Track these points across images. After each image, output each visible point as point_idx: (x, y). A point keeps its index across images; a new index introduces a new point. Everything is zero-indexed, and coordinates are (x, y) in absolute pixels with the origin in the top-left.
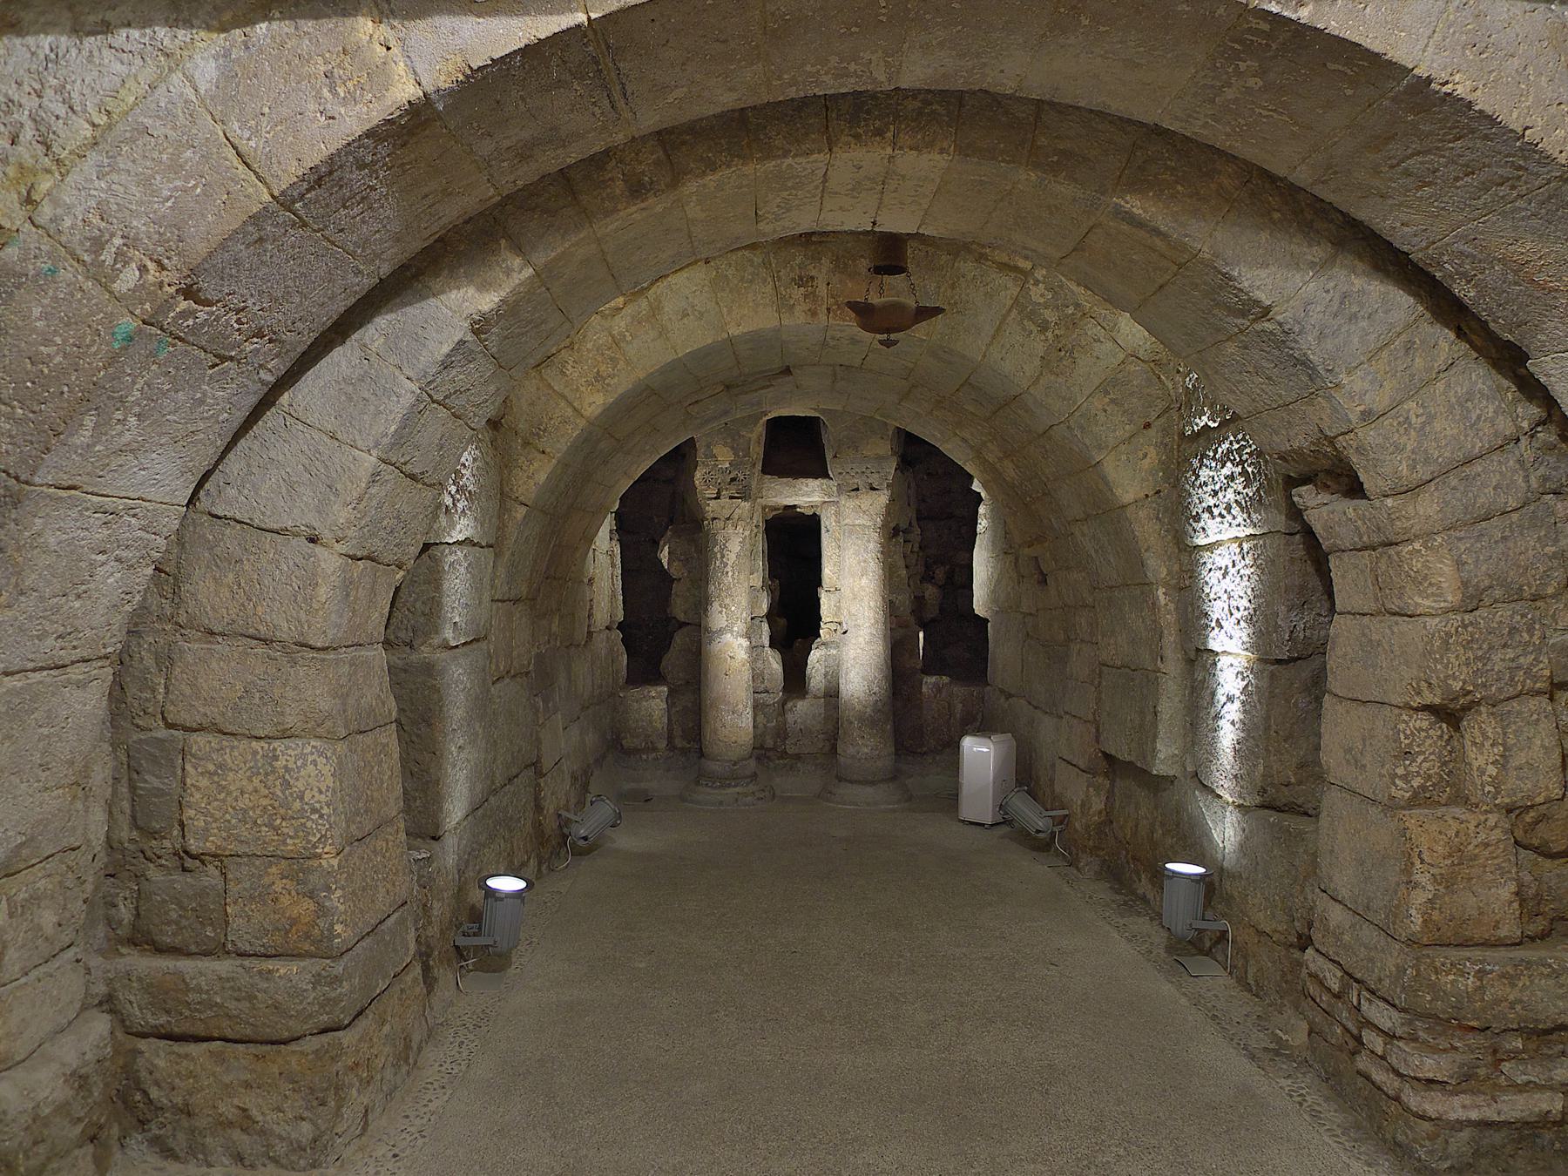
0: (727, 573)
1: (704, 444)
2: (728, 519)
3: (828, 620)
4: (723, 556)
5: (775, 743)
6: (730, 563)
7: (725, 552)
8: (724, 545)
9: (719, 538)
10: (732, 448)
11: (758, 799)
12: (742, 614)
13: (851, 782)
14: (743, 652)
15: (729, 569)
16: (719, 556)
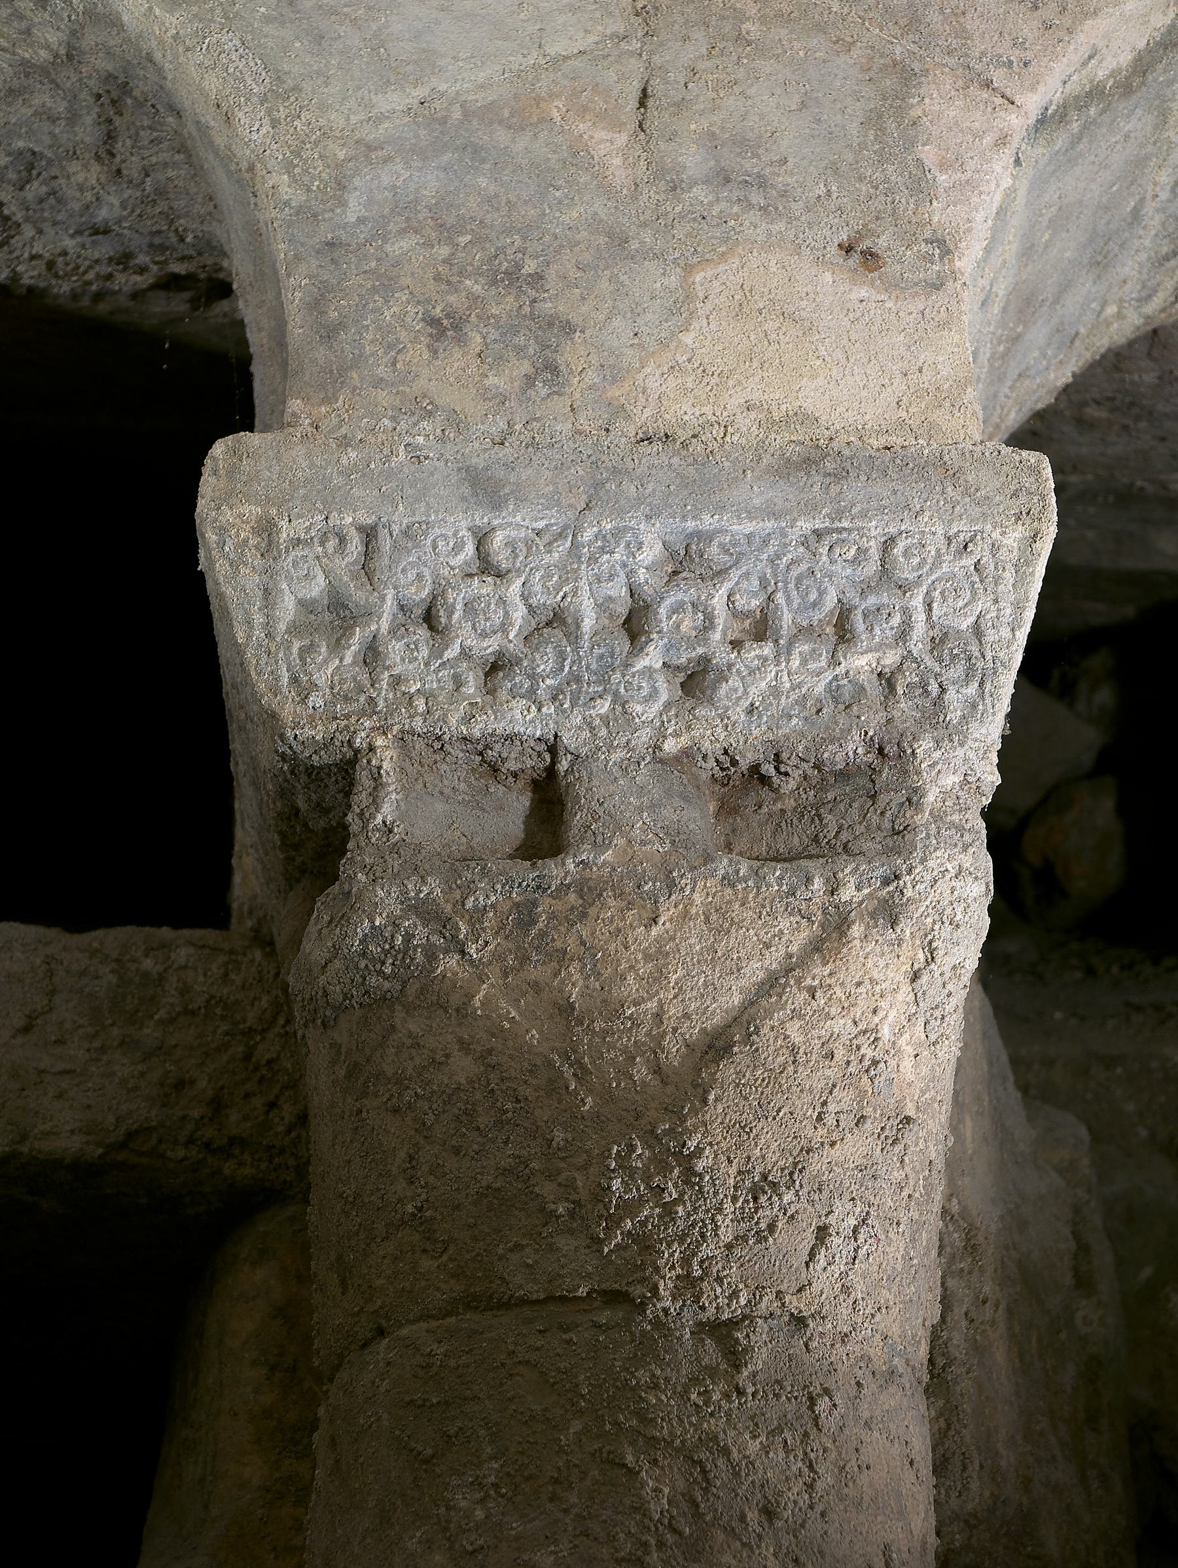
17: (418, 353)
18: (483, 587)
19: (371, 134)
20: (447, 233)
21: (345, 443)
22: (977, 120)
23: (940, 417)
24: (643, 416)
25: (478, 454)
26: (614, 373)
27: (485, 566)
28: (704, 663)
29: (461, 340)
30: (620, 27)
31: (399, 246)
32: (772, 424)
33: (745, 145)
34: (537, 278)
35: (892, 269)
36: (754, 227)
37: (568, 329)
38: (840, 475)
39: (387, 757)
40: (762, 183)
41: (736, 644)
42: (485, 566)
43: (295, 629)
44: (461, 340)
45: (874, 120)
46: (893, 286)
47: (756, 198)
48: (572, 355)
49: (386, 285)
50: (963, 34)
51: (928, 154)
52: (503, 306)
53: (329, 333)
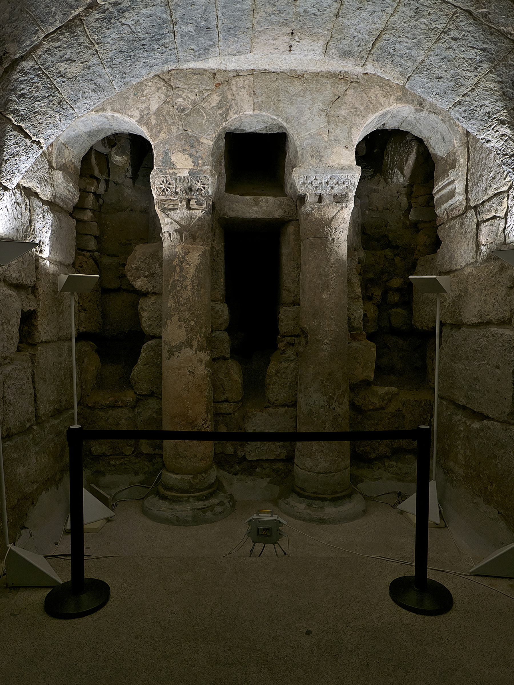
0: (186, 287)
10: (191, 156)
15: (188, 282)
16: (178, 269)
17: (310, 159)
18: (315, 180)
19: (306, 137)
21: (305, 168)
22: (357, 132)
23: (352, 163)
24: (328, 165)
26: (326, 160)
27: (316, 179)
28: (333, 186)
30: (326, 124)
32: (339, 165)
33: (337, 137)
35: (349, 149)
38: (344, 170)
39: (308, 195)
41: (335, 184)
42: (316, 179)
43: (301, 185)
44: (314, 158)
45: (348, 133)
48: (322, 159)
49: (307, 152)
50: (356, 123)
51: (352, 136)
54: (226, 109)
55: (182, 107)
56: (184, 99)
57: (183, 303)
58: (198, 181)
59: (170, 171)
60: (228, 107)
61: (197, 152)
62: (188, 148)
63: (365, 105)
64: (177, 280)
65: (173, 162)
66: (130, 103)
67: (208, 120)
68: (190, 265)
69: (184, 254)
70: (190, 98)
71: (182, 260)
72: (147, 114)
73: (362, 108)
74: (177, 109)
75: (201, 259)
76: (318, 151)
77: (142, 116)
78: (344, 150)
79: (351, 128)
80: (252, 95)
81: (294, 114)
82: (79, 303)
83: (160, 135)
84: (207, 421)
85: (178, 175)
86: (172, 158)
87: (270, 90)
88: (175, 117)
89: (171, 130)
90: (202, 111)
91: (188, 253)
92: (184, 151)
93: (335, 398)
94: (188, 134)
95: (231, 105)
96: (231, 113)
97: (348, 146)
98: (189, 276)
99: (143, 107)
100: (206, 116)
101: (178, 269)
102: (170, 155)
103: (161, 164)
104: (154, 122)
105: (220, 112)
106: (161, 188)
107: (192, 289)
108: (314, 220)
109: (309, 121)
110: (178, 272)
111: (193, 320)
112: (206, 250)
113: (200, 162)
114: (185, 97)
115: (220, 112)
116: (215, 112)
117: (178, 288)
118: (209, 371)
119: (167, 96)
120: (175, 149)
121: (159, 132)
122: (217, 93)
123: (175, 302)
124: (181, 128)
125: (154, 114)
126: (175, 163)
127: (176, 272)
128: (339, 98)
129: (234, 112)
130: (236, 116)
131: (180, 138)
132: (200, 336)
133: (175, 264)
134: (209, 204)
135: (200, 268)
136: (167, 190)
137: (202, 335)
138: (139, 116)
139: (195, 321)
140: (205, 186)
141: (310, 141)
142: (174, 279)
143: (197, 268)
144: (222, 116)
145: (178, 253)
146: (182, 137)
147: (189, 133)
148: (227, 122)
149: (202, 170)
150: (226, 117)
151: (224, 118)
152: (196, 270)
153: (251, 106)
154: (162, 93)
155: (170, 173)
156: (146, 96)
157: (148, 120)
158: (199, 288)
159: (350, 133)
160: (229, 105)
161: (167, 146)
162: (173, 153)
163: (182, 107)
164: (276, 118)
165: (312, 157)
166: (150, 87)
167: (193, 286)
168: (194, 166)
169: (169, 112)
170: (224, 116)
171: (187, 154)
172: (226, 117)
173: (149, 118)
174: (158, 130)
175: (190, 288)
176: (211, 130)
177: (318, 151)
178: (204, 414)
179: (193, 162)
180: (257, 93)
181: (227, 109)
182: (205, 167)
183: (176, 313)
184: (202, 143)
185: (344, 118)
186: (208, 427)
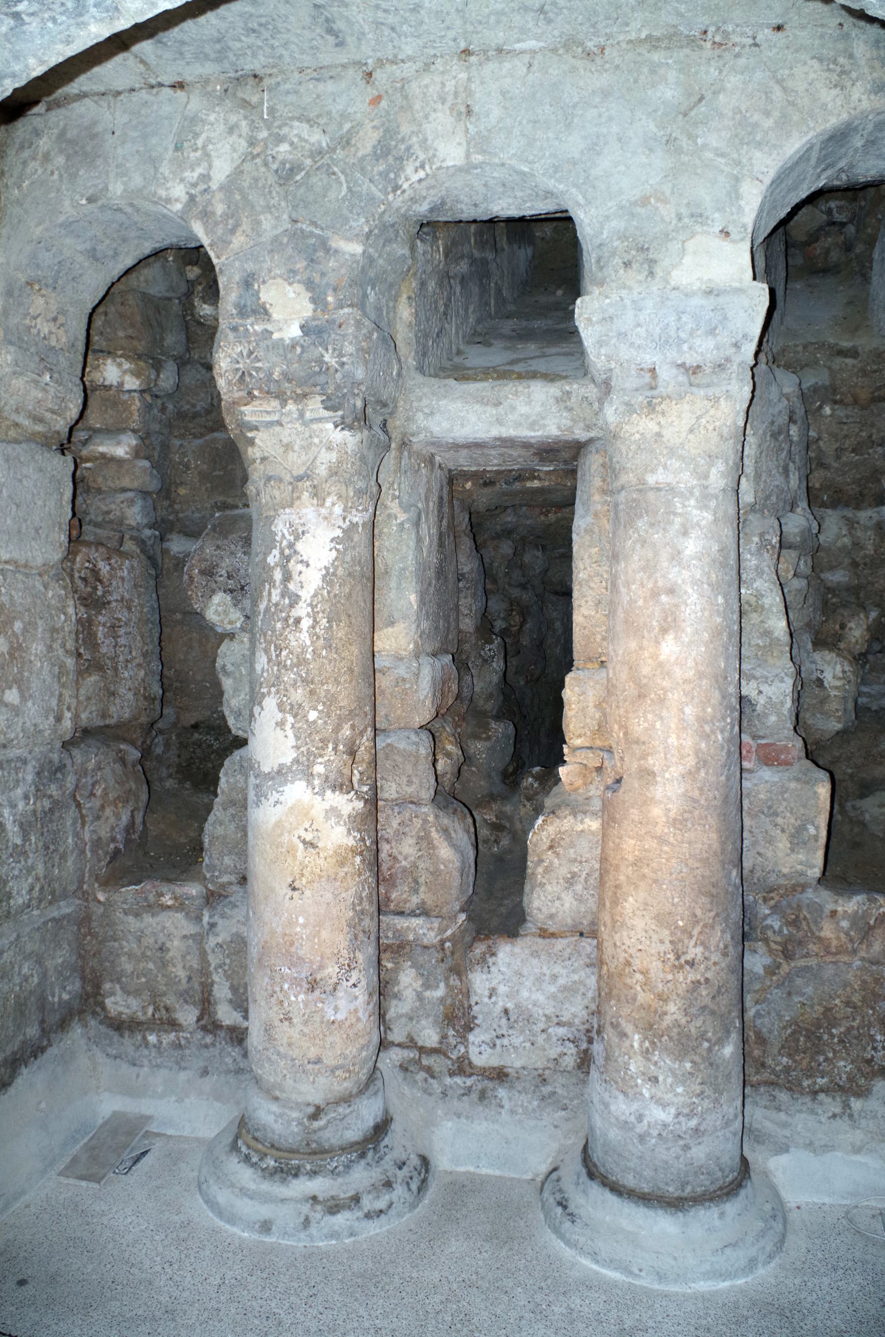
0: (298, 621)
1: (237, 278)
2: (300, 479)
3: (578, 742)
4: (287, 577)
5: (444, 1037)
6: (306, 595)
7: (295, 567)
8: (291, 546)
9: (280, 527)
10: (310, 285)
11: (368, 1216)
12: (337, 729)
13: (616, 1189)
14: (341, 830)
15: (302, 610)
16: (278, 575)
17: (622, 271)
20: (627, 238)
24: (673, 283)
25: (635, 296)
29: (631, 267)
31: (616, 243)
34: (648, 249)
35: (733, 236)
36: (698, 228)
37: (655, 262)
38: (717, 295)
40: (701, 215)
44: (631, 267)
46: (734, 242)
47: (700, 220)
49: (613, 254)
52: (641, 257)
53: (601, 268)
54: (396, 159)
55: (288, 166)
56: (292, 144)
57: (289, 662)
58: (327, 350)
59: (256, 327)
60: (401, 153)
61: (323, 274)
62: (301, 265)
63: (776, 114)
64: (277, 605)
65: (264, 303)
66: (165, 169)
67: (350, 189)
68: (308, 566)
69: (292, 538)
70: (306, 141)
71: (287, 552)
72: (205, 190)
73: (769, 123)
74: (277, 171)
75: (337, 550)
76: (642, 248)
77: (192, 198)
78: (718, 243)
79: (737, 179)
80: (463, 117)
81: (577, 156)
82: (79, 655)
83: (235, 241)
84: (350, 969)
85: (276, 336)
86: (261, 295)
87: (511, 98)
88: (270, 192)
89: (259, 223)
90: (336, 169)
91: (303, 533)
92: (291, 276)
93: (695, 932)
94: (302, 231)
95: (408, 149)
96: (409, 169)
97: (729, 229)
98: (306, 595)
99: (195, 175)
100: (347, 182)
101: (278, 575)
102: (256, 287)
103: (234, 311)
104: (220, 209)
105: (382, 168)
106: (237, 370)
107: (313, 627)
108: (637, 436)
109: (619, 168)
110: (278, 583)
111: (315, 709)
112: (353, 526)
113: (330, 299)
114: (296, 140)
115: (381, 168)
116: (369, 168)
117: (279, 625)
118: (363, 840)
119: (252, 142)
120: (270, 271)
121: (233, 231)
122: (372, 121)
123: (270, 660)
124: (285, 216)
125: (221, 188)
126: (268, 306)
127: (274, 586)
128: (704, 102)
129: (418, 164)
130: (422, 174)
131: (281, 244)
132: (335, 749)
133: (272, 564)
134: (355, 405)
135: (334, 574)
136: (251, 375)
137: (341, 747)
138: (184, 198)
139: (320, 712)
140: (344, 359)
141: (616, 224)
142: (269, 601)
143: (328, 573)
144: (386, 176)
145: (280, 534)
146: (285, 240)
147: (304, 226)
148: (399, 192)
149: (334, 321)
150: (395, 179)
151: (390, 181)
152: (324, 577)
153: (459, 144)
154: (240, 136)
155: (255, 333)
156: (204, 147)
157: (206, 206)
158: (331, 627)
159: (735, 195)
160: (403, 147)
161: (250, 266)
162: (264, 282)
163: (288, 166)
164: (526, 169)
165: (627, 265)
166: (212, 125)
167: (315, 620)
168: (315, 311)
169: (256, 180)
170: (392, 175)
171: (299, 282)
172: (395, 179)
173: (210, 200)
174: (230, 227)
175: (306, 623)
176: (358, 214)
177: (642, 248)
178: (345, 953)
179: (313, 300)
180: (476, 109)
181: (400, 159)
182: (342, 312)
183: (273, 690)
184: (336, 251)
185: (718, 155)
186: (355, 985)
